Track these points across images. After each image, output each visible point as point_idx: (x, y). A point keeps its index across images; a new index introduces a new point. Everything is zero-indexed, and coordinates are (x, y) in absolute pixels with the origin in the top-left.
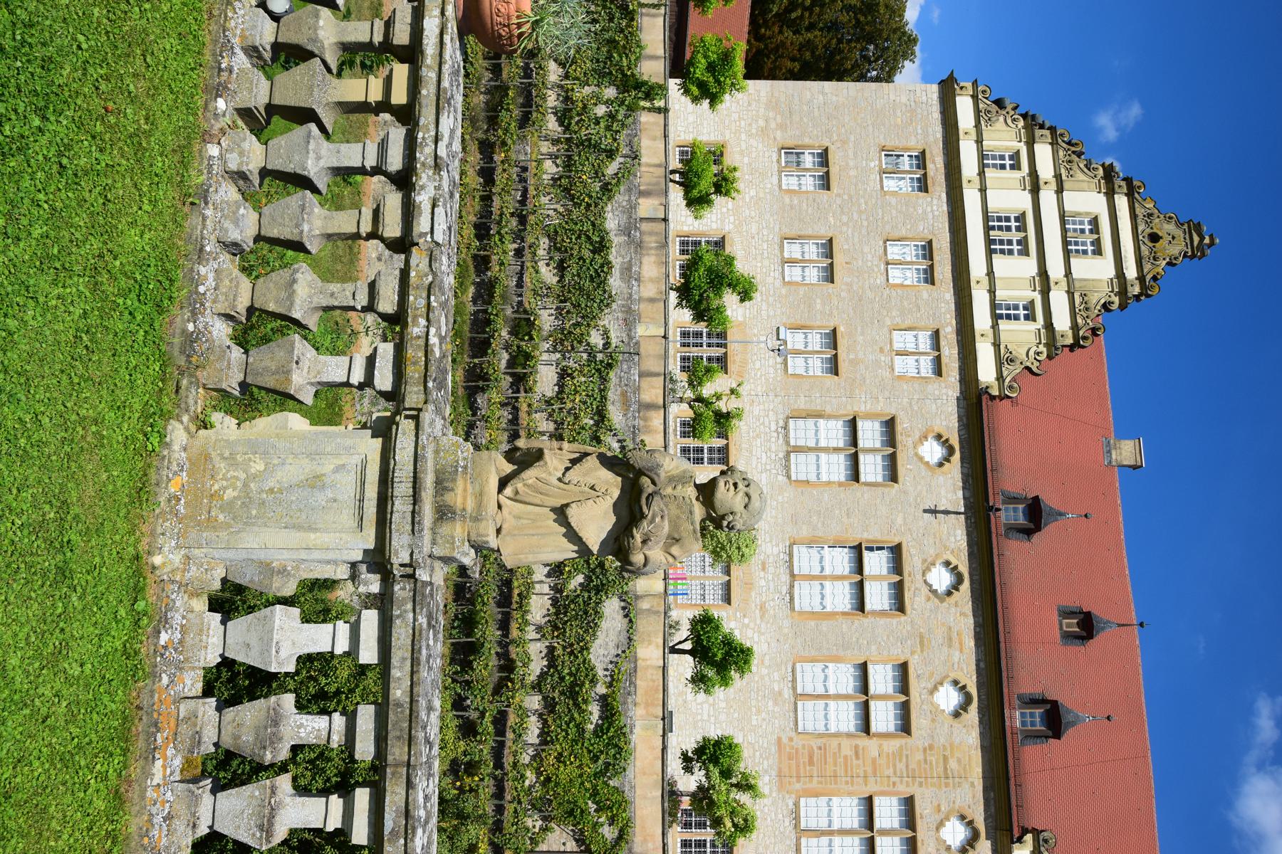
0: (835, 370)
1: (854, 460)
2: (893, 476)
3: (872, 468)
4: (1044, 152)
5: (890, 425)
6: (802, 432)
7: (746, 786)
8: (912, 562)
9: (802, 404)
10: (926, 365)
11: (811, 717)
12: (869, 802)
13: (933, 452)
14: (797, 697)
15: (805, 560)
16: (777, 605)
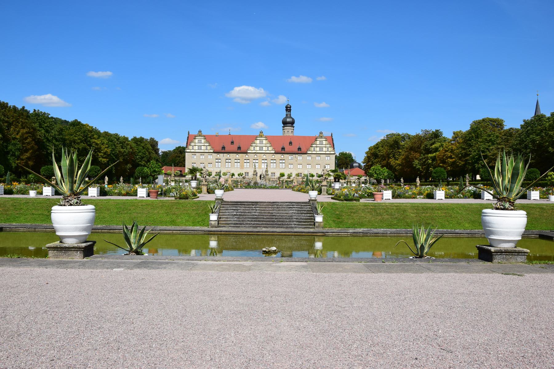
0: (212, 163)
1: (219, 162)
2: (220, 159)
3: (220, 161)
4: (192, 144)
5: (216, 159)
6: (217, 166)
7: (240, 173)
8: (227, 158)
9: (214, 166)
10: (211, 156)
11: (239, 166)
12: (245, 162)
13: (218, 156)
14: (237, 167)
15: (227, 166)
16: (230, 169)
